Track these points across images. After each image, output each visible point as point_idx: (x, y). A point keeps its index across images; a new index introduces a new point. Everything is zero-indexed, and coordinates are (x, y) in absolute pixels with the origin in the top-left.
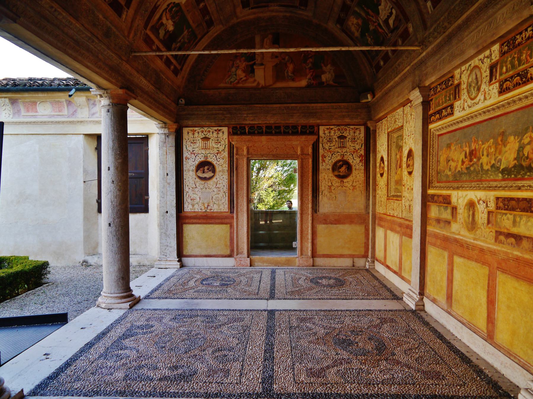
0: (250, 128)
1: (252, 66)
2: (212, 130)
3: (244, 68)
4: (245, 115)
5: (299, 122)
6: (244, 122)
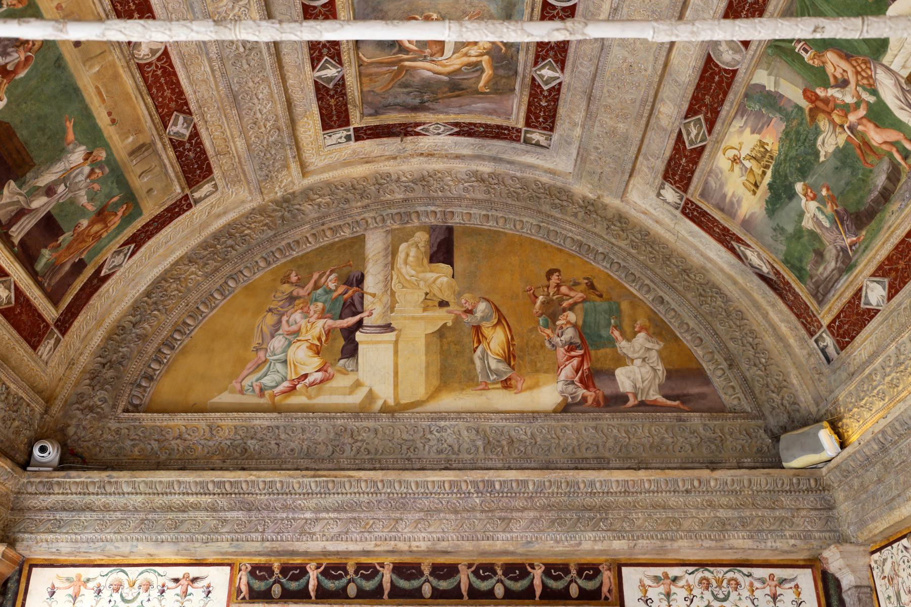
0: (327, 572)
1: (349, 334)
2: (161, 580)
3: (319, 339)
4: (308, 515)
5: (536, 547)
6: (301, 546)
